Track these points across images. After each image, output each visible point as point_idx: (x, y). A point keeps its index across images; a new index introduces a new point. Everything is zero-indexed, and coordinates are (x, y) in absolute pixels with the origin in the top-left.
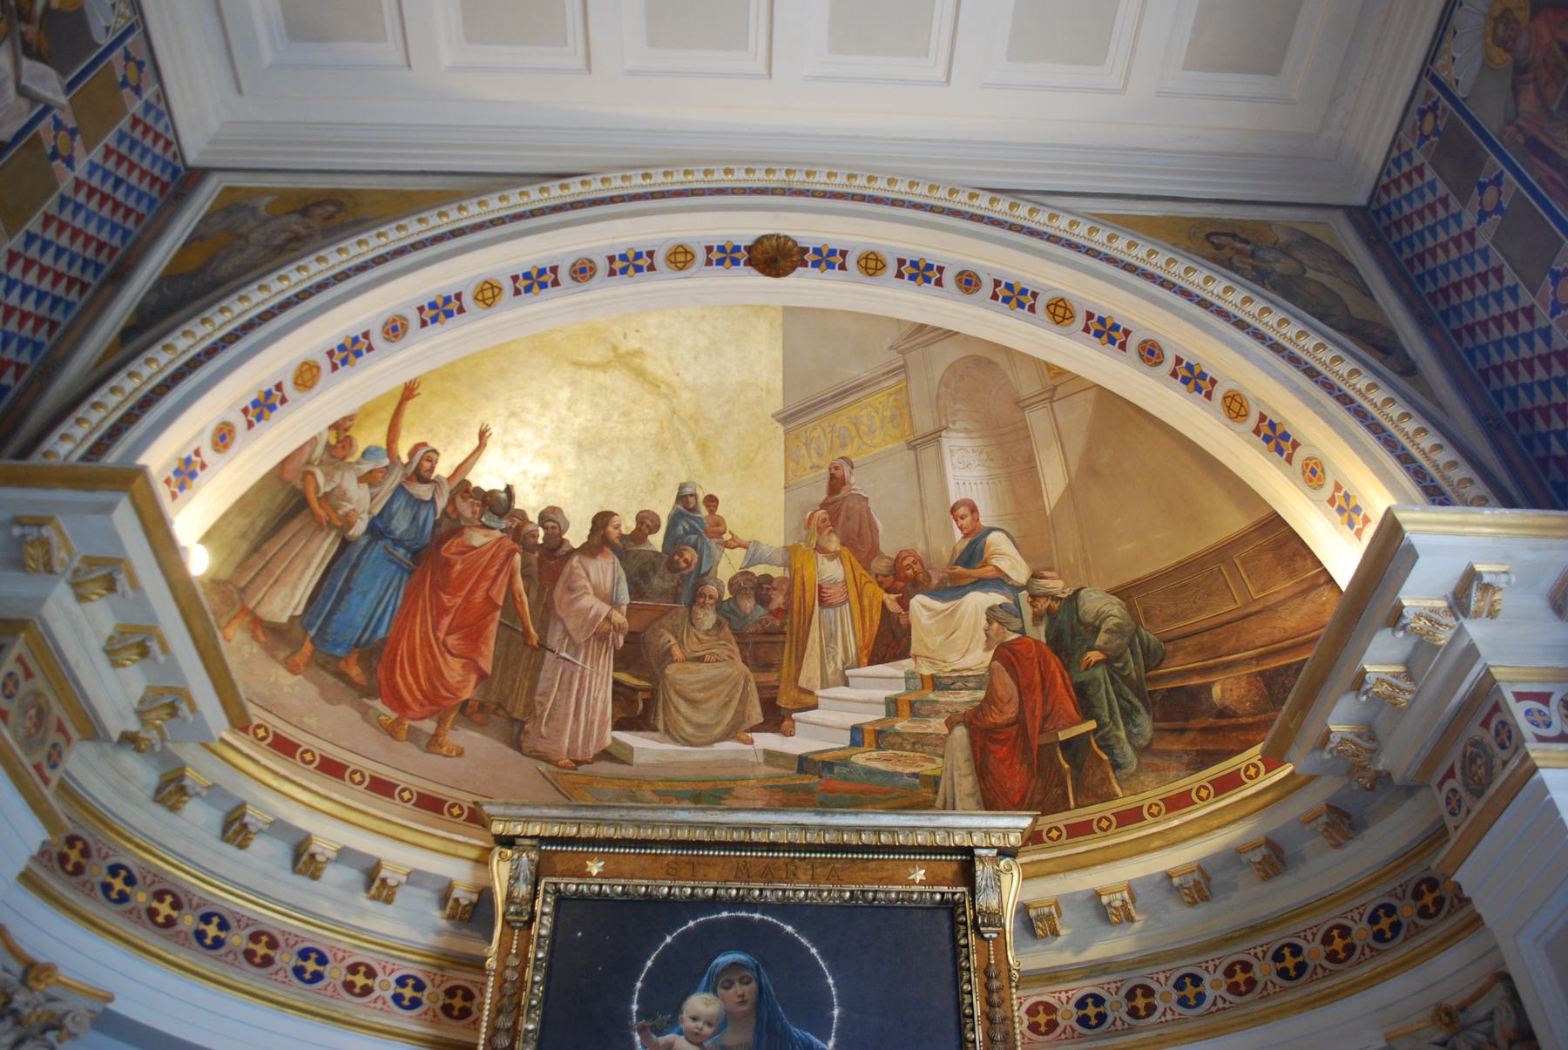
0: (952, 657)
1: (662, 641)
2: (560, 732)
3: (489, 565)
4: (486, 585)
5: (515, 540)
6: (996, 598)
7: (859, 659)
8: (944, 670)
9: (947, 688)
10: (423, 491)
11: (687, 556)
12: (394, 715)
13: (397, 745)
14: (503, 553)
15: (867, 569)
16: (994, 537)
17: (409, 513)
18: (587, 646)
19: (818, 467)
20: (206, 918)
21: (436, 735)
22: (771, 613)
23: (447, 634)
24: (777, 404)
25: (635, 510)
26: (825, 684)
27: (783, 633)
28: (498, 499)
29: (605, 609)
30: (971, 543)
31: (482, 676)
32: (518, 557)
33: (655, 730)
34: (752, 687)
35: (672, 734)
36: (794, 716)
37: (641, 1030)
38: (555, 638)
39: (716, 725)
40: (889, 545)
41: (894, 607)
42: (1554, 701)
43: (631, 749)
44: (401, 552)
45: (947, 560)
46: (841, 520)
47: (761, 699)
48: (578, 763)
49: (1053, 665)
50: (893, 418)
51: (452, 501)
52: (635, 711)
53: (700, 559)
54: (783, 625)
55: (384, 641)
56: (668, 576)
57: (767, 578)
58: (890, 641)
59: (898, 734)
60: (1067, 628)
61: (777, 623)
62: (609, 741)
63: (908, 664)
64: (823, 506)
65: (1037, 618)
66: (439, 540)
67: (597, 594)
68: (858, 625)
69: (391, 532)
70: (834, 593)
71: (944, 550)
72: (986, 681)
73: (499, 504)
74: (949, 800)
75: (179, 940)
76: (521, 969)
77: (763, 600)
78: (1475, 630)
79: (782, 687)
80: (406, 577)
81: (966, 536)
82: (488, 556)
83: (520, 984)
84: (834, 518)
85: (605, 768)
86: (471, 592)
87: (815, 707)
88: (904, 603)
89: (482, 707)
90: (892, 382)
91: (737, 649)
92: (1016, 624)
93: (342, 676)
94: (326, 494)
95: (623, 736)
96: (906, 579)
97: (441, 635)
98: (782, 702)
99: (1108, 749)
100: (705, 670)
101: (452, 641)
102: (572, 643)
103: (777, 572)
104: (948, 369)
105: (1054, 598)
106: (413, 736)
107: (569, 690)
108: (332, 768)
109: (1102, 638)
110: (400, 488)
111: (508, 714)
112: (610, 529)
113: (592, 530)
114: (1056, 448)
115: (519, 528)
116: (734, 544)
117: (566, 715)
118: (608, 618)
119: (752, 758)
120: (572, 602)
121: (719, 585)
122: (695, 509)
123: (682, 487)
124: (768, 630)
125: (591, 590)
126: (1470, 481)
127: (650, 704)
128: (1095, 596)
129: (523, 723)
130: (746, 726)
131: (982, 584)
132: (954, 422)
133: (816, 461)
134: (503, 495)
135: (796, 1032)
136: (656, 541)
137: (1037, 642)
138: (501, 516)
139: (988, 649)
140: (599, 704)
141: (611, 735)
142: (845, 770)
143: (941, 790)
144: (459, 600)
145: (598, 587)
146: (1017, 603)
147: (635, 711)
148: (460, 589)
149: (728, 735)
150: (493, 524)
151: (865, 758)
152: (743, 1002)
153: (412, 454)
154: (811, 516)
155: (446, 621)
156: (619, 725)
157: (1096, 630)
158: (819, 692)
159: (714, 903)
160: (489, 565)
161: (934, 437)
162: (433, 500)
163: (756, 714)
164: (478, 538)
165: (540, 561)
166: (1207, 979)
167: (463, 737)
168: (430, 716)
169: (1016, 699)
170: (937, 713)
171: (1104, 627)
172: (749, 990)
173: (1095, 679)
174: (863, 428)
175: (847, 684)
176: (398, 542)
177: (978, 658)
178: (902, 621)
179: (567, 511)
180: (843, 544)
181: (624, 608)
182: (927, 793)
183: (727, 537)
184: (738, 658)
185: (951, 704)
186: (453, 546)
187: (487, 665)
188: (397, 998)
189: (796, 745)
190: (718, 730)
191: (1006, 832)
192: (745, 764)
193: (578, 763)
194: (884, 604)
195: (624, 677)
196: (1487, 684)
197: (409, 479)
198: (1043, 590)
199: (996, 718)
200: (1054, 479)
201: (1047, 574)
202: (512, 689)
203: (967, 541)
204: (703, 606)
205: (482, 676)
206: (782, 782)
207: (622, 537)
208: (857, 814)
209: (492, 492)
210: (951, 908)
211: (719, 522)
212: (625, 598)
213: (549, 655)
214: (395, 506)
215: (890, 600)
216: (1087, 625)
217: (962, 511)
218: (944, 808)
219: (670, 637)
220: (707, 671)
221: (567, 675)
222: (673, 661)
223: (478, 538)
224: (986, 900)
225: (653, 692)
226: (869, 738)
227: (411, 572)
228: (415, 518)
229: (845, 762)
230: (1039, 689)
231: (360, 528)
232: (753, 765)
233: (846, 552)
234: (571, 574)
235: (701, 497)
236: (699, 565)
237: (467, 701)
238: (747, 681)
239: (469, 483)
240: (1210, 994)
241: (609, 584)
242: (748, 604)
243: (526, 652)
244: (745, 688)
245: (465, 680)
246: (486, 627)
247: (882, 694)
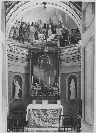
6: (62, 29)
9: (58, 36)
10: (19, 23)
26: (49, 36)
31: (26, 37)
40: (54, 24)
63: (55, 34)
64: (49, 21)
65: (65, 31)
85: (34, 43)
88: (55, 29)
95: (35, 41)
96: (56, 27)
101: (23, 35)
127: (37, 38)
141: (35, 41)
145: (32, 29)
147: (36, 39)
164: (23, 26)
177: (61, 34)
189: (48, 41)
195: (35, 36)
205: (26, 37)
212: (35, 29)
231: (16, 28)
247: (53, 37)
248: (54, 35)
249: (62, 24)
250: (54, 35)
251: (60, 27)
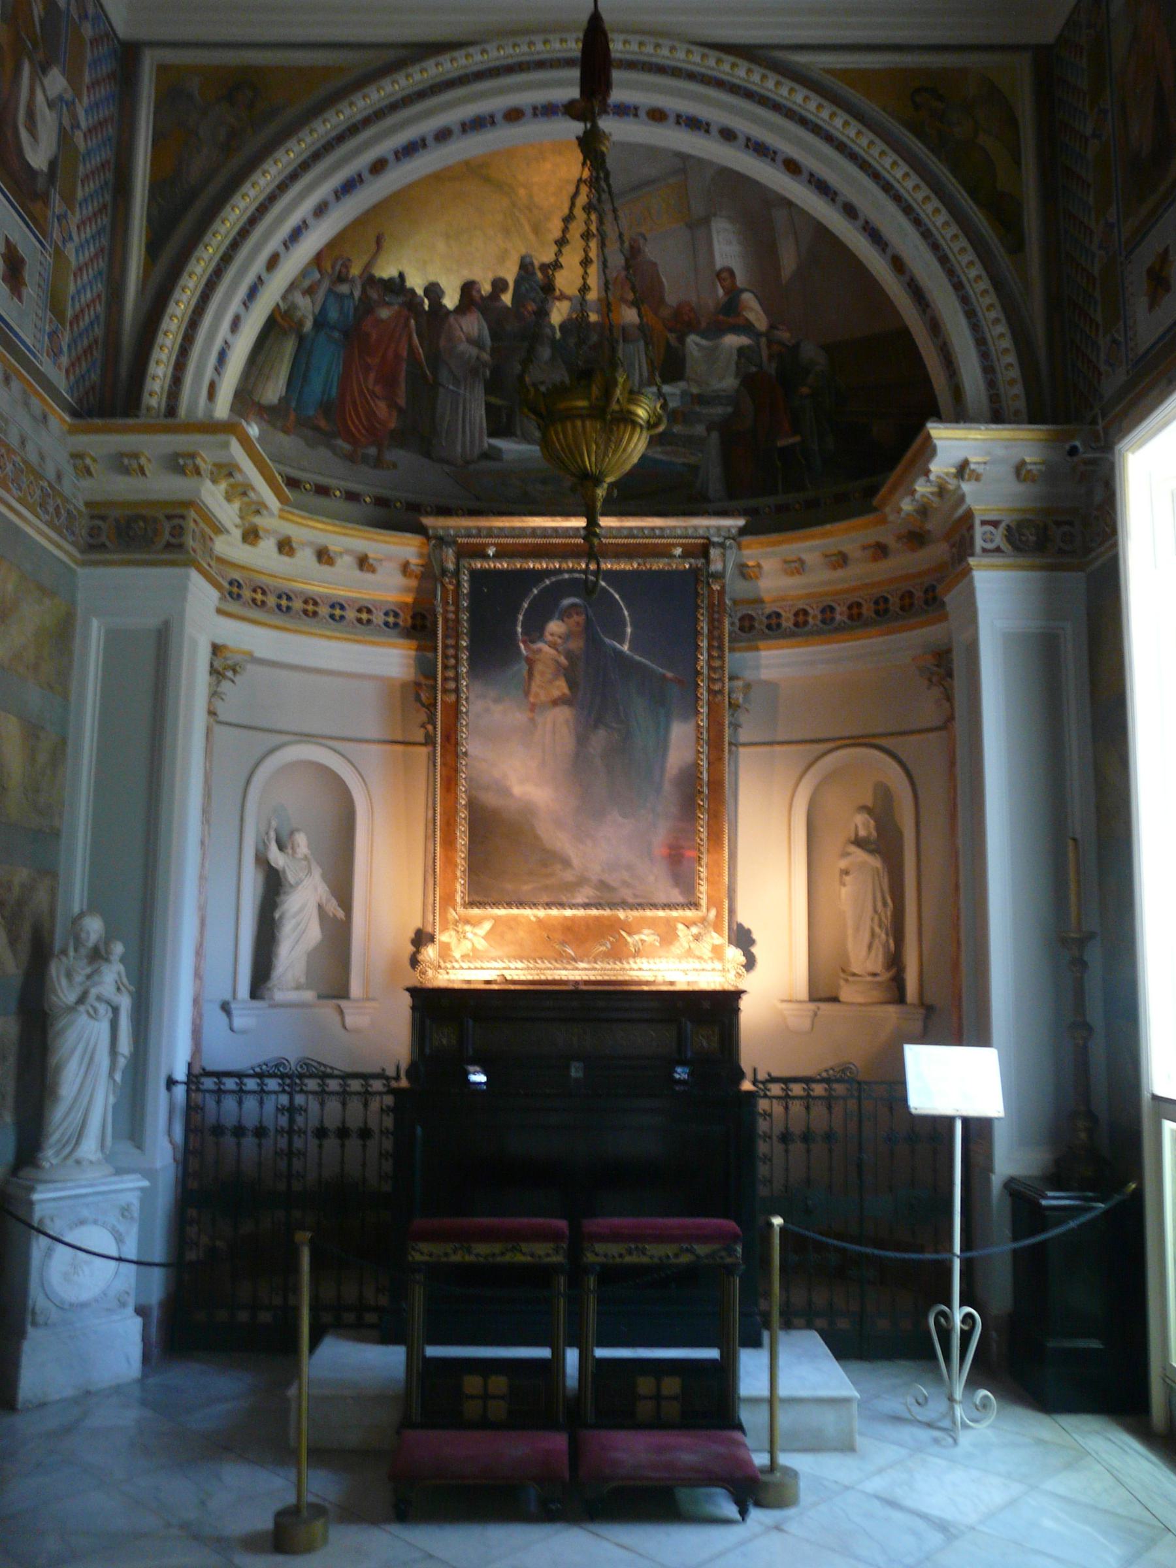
6: (743, 340)
10: (344, 289)
20: (280, 597)
25: (490, 276)
29: (474, 351)
32: (412, 322)
37: (524, 642)
38: (444, 375)
40: (672, 298)
42: (1003, 525)
43: (500, 450)
48: (468, 463)
51: (364, 291)
58: (671, 367)
62: (486, 445)
63: (682, 385)
65: (771, 357)
73: (397, 286)
75: (270, 611)
76: (456, 612)
78: (966, 487)
83: (457, 621)
88: (681, 340)
93: (317, 429)
94: (286, 312)
95: (498, 442)
96: (684, 321)
106: (365, 459)
108: (322, 490)
110: (330, 291)
112: (474, 293)
113: (461, 296)
121: (552, 327)
122: (534, 274)
123: (523, 259)
126: (1011, 365)
131: (736, 329)
134: (398, 280)
135: (607, 640)
136: (507, 298)
139: (737, 375)
152: (578, 623)
153: (333, 267)
155: (372, 375)
156: (492, 434)
159: (559, 571)
161: (706, 221)
162: (352, 293)
164: (384, 313)
166: (838, 609)
167: (395, 455)
172: (580, 619)
176: (333, 328)
177: (729, 383)
179: (443, 284)
181: (488, 350)
183: (557, 293)
188: (386, 624)
191: (729, 529)
193: (468, 463)
195: (493, 400)
196: (969, 515)
205: (400, 411)
209: (391, 280)
210: (694, 572)
212: (488, 342)
217: (725, 275)
223: (384, 313)
224: (716, 566)
228: (342, 308)
231: (308, 325)
240: (838, 617)
241: (476, 330)
249: (747, 297)
251: (728, 316)
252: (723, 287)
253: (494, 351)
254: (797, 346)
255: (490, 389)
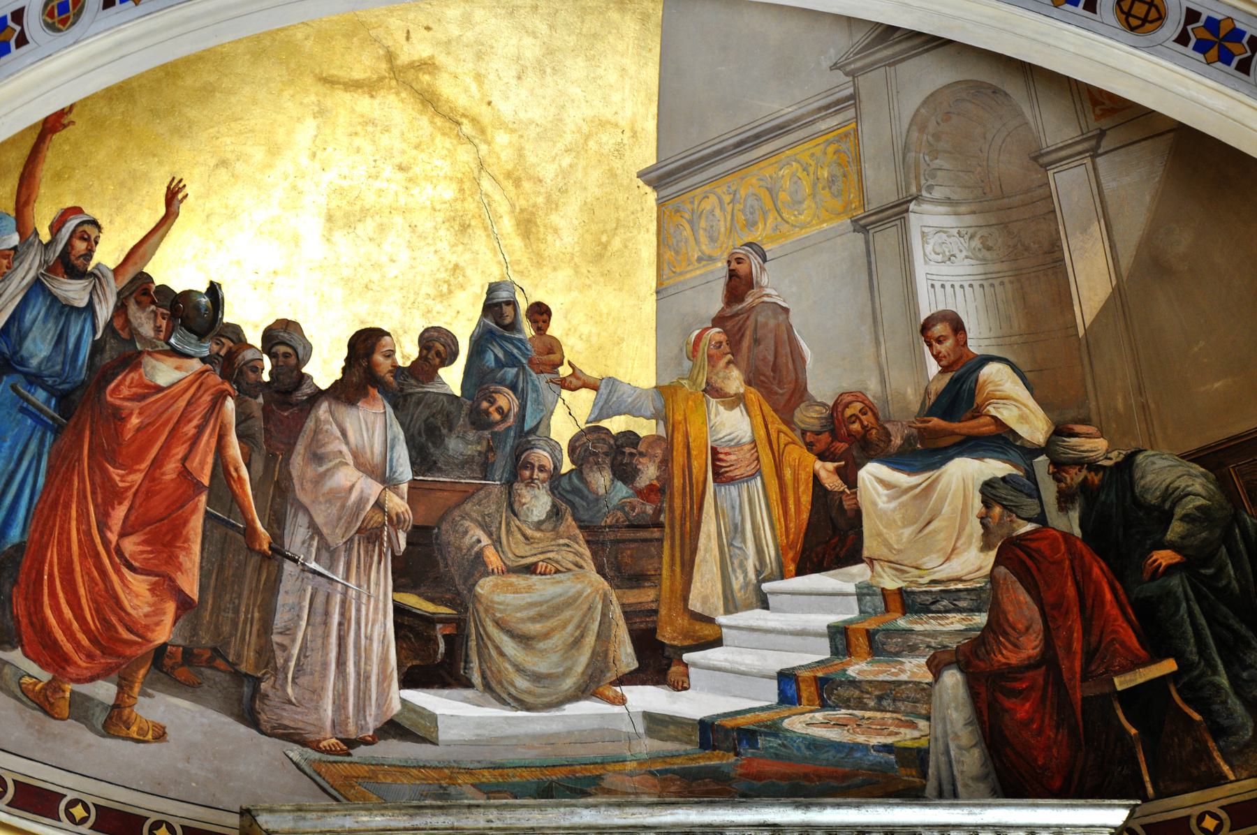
0: (931, 561)
1: (467, 540)
2: (317, 693)
3: (184, 418)
4: (180, 451)
5: (225, 376)
6: (996, 468)
7: (781, 566)
8: (920, 582)
9: (925, 609)
10: (74, 291)
11: (502, 402)
12: (45, 676)
13: (55, 726)
14: (207, 398)
15: (789, 422)
16: (991, 371)
17: (52, 330)
18: (349, 551)
19: (711, 259)
21: (117, 706)
22: (639, 493)
23: (122, 535)
24: (647, 156)
27: (660, 526)
28: (197, 306)
29: (374, 489)
30: (953, 382)
31: (184, 604)
32: (230, 404)
33: (468, 685)
34: (616, 611)
35: (495, 691)
36: (686, 657)
38: (297, 538)
39: (565, 674)
40: (823, 384)
41: (832, 482)
43: (433, 718)
44: (40, 396)
45: (916, 407)
46: (746, 343)
47: (632, 633)
48: (351, 743)
49: (1096, 571)
50: (832, 181)
51: (121, 308)
52: (434, 655)
53: (523, 407)
54: (659, 511)
55: (20, 548)
56: (471, 435)
57: (630, 438)
58: (829, 537)
59: (853, 683)
60: (1116, 511)
61: (649, 509)
62: (396, 707)
63: (860, 572)
64: (718, 321)
65: (1065, 500)
66: (102, 375)
67: (359, 465)
68: (777, 511)
69: (23, 362)
70: (737, 462)
71: (910, 391)
72: (987, 596)
73: (198, 314)
74: (947, 787)
77: (624, 473)
79: (663, 612)
80: (49, 437)
81: (945, 370)
82: (182, 403)
84: (734, 342)
85: (395, 750)
86: (157, 463)
87: (717, 642)
88: (849, 477)
89: (189, 656)
90: (833, 122)
91: (587, 553)
92: (1032, 508)
95: (421, 698)
96: (851, 437)
97: (113, 537)
98: (667, 635)
99: (1202, 705)
100: (540, 587)
101: (130, 546)
102: (324, 546)
103: (645, 428)
104: (925, 103)
105: (1093, 466)
106: (81, 709)
107: (326, 623)
109: (1176, 529)
110: (37, 287)
111: (231, 668)
112: (378, 358)
113: (347, 360)
114: (1097, 230)
115: (231, 356)
116: (578, 381)
117: (325, 665)
118: (379, 505)
119: (626, 728)
120: (320, 479)
121: (554, 448)
122: (514, 326)
123: (493, 289)
124: (635, 516)
125: (349, 459)
127: (456, 642)
128: (1160, 463)
129: (259, 680)
130: (611, 676)
131: (973, 445)
132: (930, 188)
133: (707, 249)
134: (205, 300)
136: (452, 377)
137: (1067, 537)
138: (201, 336)
139: (986, 547)
140: (376, 646)
141: (398, 697)
142: (774, 742)
143: (931, 771)
144: (137, 478)
146: (1031, 475)
147: (434, 655)
148: (139, 458)
149: (588, 689)
150: (188, 349)
151: (805, 723)
153: (56, 228)
154: (699, 337)
155: (119, 513)
156: (408, 681)
157: (1167, 517)
158: (722, 619)
160: (184, 418)
162: (90, 307)
163: (626, 656)
164: (165, 373)
165: (265, 409)
168: (104, 674)
169: (1038, 625)
170: (913, 650)
171: (1179, 512)
173: (1170, 593)
174: (783, 196)
175: (765, 606)
176: (35, 379)
177: (972, 562)
178: (847, 504)
180: (749, 383)
181: (404, 488)
182: (909, 776)
183: (565, 371)
184: (590, 566)
185: (933, 634)
186: (120, 391)
187: (190, 585)
189: (695, 704)
190: (568, 684)
192: (616, 737)
193: (351, 743)
194: (816, 478)
197: (51, 270)
198: (1073, 455)
199: (1010, 657)
200: (1092, 280)
201: (1079, 428)
202: (235, 624)
203: (947, 378)
204: (531, 482)
205: (184, 604)
206: (678, 764)
207: (397, 370)
208: (858, 806)
209: (187, 294)
211: (553, 347)
212: (405, 472)
213: (288, 566)
214: (29, 318)
215: (827, 471)
216: (1149, 509)
217: (939, 329)
218: (941, 795)
219: (480, 533)
220: (544, 588)
221: (320, 599)
222: (487, 573)
223: (165, 373)
225: (460, 624)
226: (807, 692)
227: (58, 430)
228: (61, 338)
229: (774, 729)
230: (1076, 610)
232: (629, 738)
233: (754, 395)
234: (316, 432)
235: (523, 306)
236: (521, 417)
237: (165, 645)
238: (606, 603)
239: (149, 279)
242: (601, 480)
243: (250, 561)
244: (604, 615)
245: (158, 611)
246: (186, 522)
247: (822, 620)
248: (817, 605)
249: (996, 376)
250: (817, 605)
251: (951, 420)
252: (936, 357)
253: (416, 492)
254: (1129, 461)
255: (408, 573)
